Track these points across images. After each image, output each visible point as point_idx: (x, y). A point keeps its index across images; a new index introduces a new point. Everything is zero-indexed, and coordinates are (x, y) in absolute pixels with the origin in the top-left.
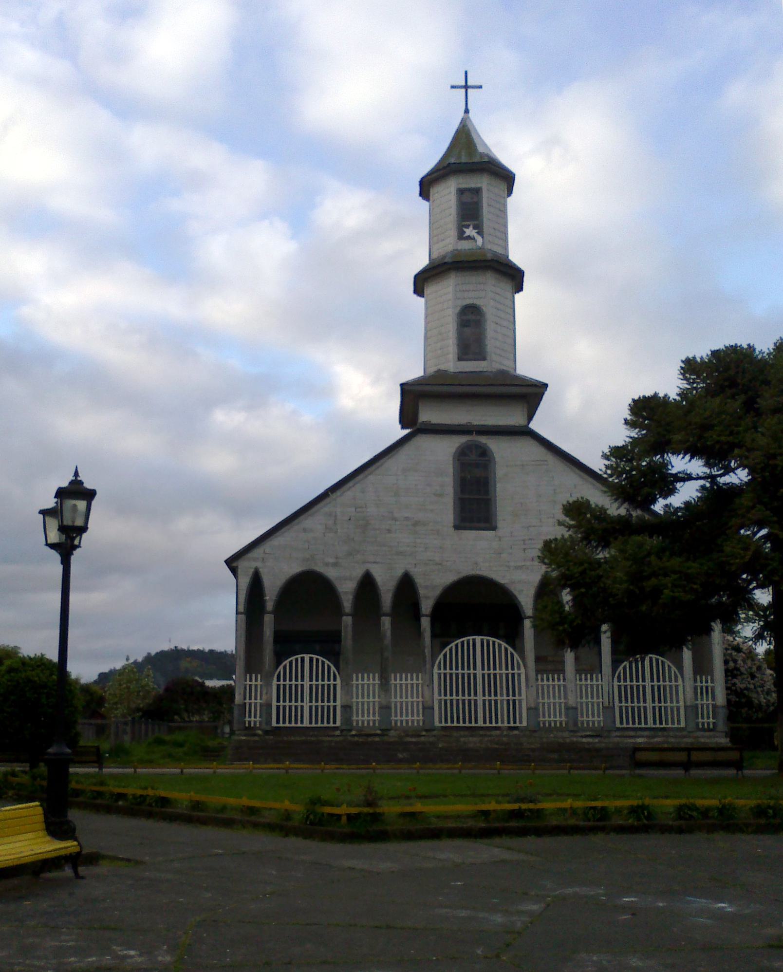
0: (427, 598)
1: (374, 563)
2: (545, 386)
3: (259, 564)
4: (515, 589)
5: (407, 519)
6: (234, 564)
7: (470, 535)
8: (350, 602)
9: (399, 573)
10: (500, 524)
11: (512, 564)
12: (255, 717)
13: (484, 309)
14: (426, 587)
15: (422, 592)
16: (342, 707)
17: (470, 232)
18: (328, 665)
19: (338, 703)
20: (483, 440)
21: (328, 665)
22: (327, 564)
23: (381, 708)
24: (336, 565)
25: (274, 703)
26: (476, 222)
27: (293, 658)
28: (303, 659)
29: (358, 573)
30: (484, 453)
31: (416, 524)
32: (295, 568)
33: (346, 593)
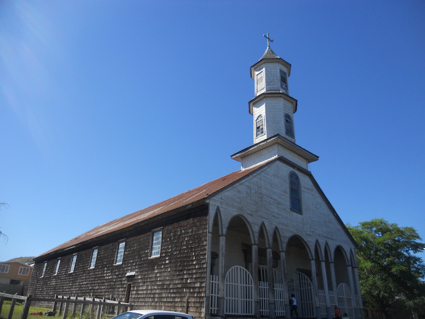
0: (284, 242)
1: (265, 218)
2: (318, 157)
3: (217, 204)
4: (309, 244)
5: (275, 200)
6: (207, 201)
7: (295, 215)
8: (257, 238)
9: (274, 227)
10: (303, 212)
11: (307, 233)
12: (214, 307)
13: (292, 117)
14: (283, 237)
15: (282, 238)
16: (255, 302)
17: (284, 86)
18: (248, 274)
19: (253, 300)
20: (297, 172)
21: (248, 274)
22: (248, 214)
23: (269, 304)
24: (251, 215)
25: (225, 298)
26: (285, 85)
27: (233, 267)
28: (237, 268)
29: (260, 223)
30: (297, 178)
31: (278, 203)
32: (235, 213)
33: (256, 232)
